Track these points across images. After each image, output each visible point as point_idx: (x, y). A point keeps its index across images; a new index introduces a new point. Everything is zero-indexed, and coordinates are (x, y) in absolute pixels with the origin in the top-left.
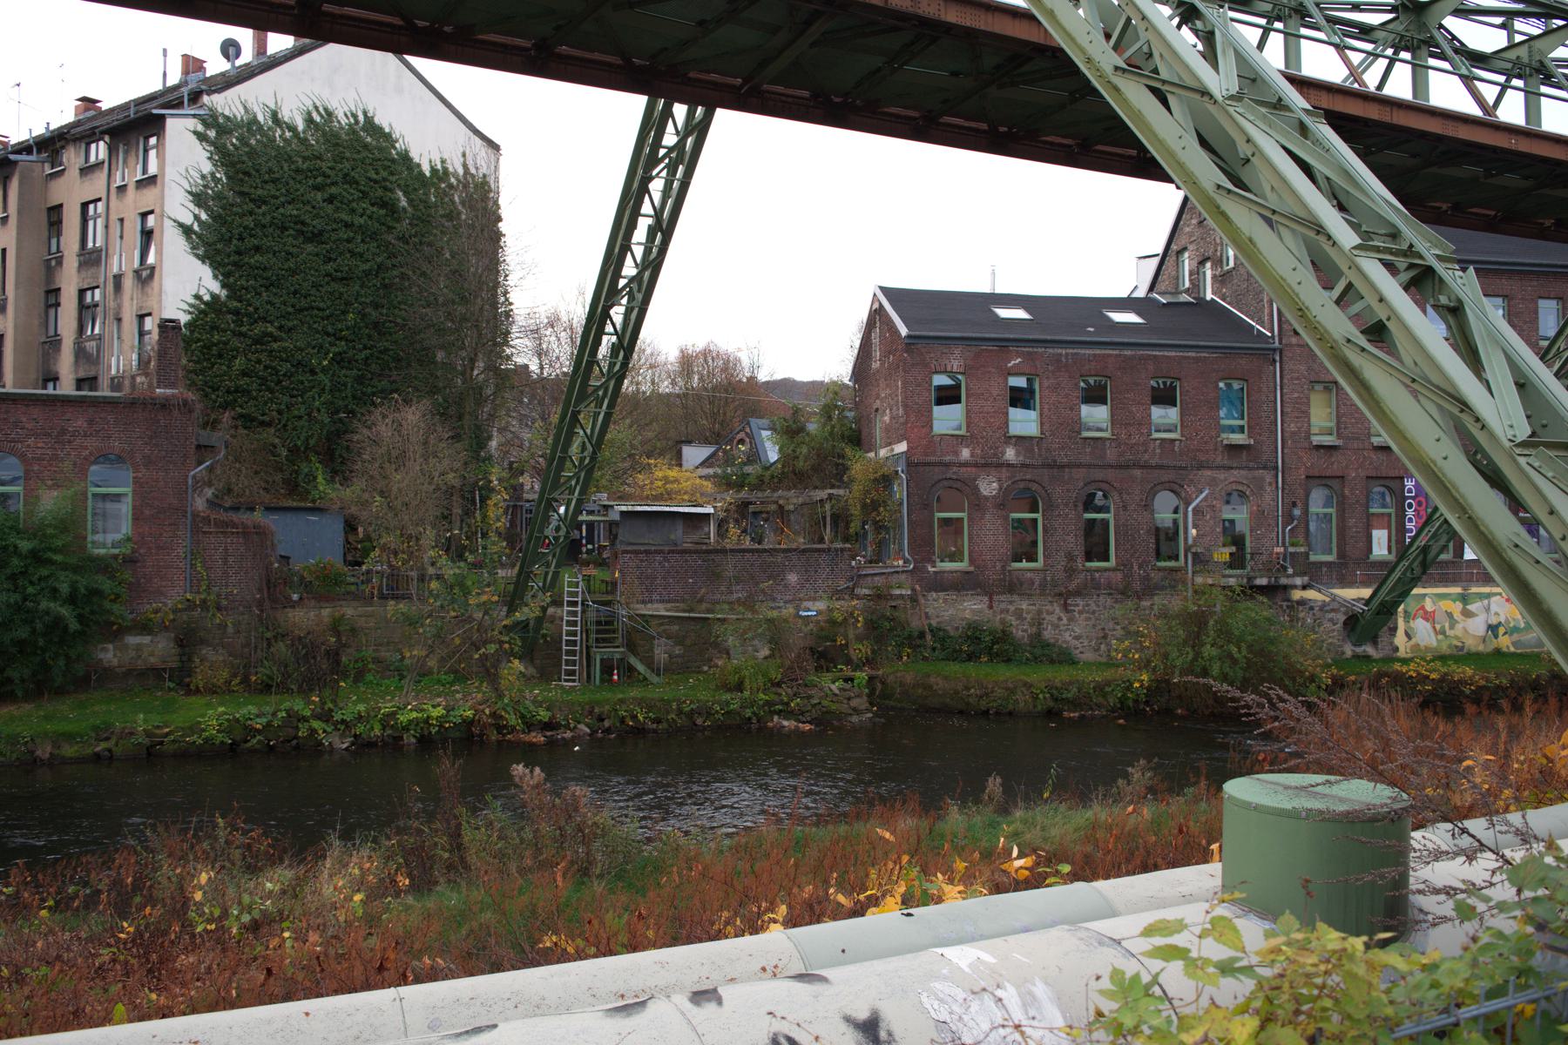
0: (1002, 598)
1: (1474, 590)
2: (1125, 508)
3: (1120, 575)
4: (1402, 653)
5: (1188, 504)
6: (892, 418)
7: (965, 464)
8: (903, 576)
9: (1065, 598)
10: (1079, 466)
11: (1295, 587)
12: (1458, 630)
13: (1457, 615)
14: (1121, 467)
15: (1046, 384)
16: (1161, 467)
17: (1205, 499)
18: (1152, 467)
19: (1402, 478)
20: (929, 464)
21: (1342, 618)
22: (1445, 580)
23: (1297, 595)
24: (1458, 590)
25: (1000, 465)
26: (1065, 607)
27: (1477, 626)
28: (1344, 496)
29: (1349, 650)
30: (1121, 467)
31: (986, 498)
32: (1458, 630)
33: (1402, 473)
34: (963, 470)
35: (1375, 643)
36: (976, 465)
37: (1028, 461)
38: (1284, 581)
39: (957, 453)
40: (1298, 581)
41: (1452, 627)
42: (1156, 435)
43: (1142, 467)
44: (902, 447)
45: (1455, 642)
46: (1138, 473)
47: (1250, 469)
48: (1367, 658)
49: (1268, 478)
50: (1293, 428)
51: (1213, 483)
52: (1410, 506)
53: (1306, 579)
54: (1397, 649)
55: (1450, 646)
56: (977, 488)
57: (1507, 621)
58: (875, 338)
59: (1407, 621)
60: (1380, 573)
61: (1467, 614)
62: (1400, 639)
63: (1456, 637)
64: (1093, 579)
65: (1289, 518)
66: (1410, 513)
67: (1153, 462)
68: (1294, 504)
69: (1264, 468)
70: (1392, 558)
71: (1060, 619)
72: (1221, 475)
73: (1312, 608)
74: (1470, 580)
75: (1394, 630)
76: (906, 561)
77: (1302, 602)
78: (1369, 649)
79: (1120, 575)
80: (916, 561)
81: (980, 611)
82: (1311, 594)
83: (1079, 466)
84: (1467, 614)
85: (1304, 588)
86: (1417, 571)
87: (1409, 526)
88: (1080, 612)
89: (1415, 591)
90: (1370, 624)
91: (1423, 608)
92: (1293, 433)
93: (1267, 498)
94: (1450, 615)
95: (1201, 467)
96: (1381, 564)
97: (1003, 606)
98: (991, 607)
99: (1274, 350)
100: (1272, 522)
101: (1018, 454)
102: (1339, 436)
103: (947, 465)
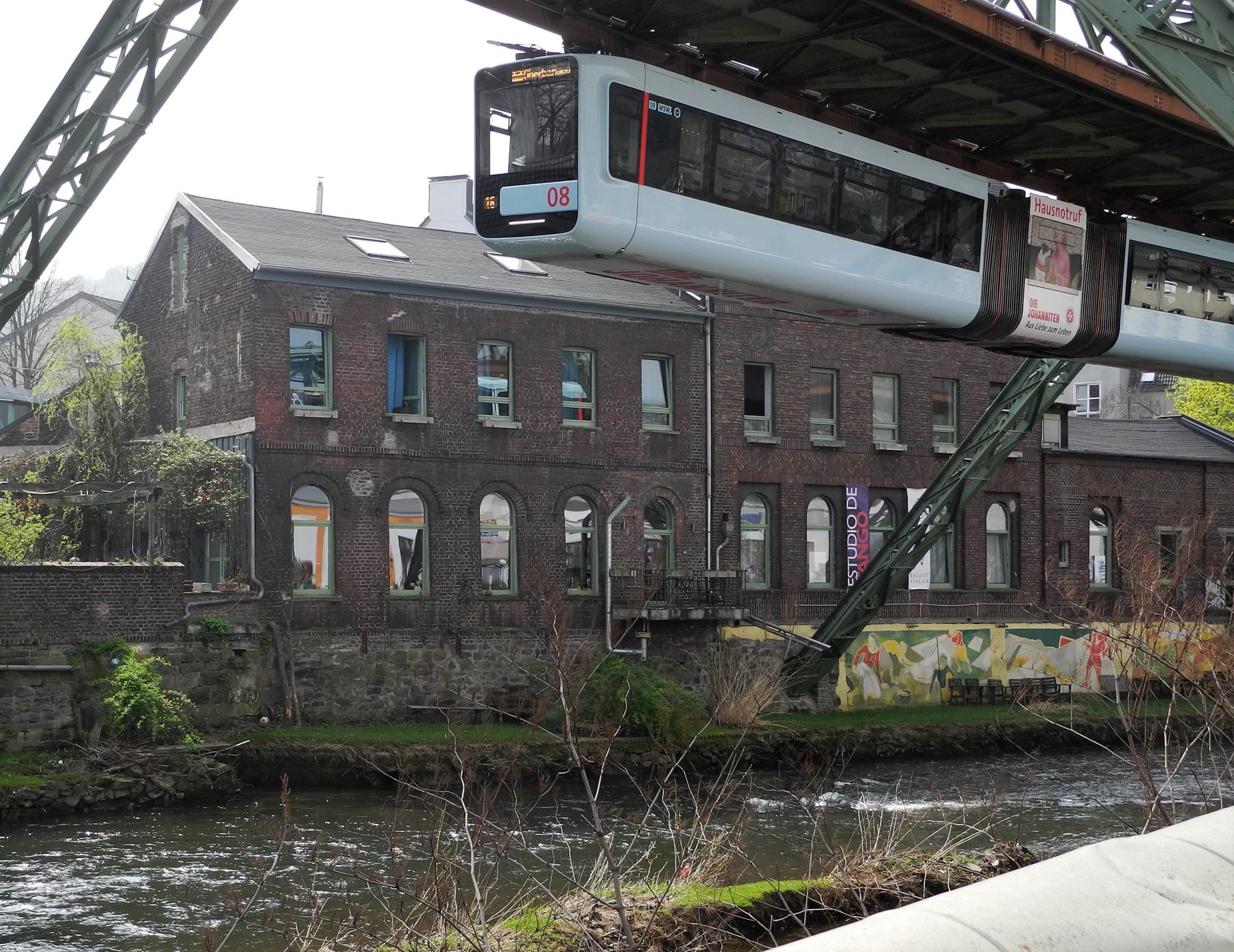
0: (380, 637)
1: (922, 627)
2: (529, 517)
3: (524, 606)
4: (844, 706)
5: (605, 514)
6: (216, 386)
7: (332, 453)
8: (250, 608)
9: (455, 636)
10: (475, 459)
11: (725, 622)
12: (902, 679)
13: (902, 658)
14: (526, 463)
15: (435, 347)
16: (572, 465)
17: (624, 510)
18: (563, 465)
19: (843, 488)
20: (284, 451)
21: (778, 664)
22: (892, 617)
23: (729, 632)
24: (900, 627)
25: (377, 456)
26: (458, 649)
27: (922, 671)
28: (780, 509)
29: (785, 703)
30: (526, 463)
31: (358, 500)
32: (902, 679)
33: (843, 481)
34: (329, 460)
35: (813, 692)
36: (346, 455)
37: (412, 452)
38: (722, 614)
39: (322, 438)
40: (738, 614)
41: (896, 673)
42: (567, 423)
43: (552, 464)
44: (248, 425)
45: (901, 692)
46: (546, 471)
47: (675, 470)
48: (806, 712)
49: (695, 479)
50: (724, 419)
51: (633, 487)
52: (852, 522)
53: (747, 610)
54: (838, 701)
55: (895, 696)
56: (347, 485)
57: (955, 666)
58: (180, 266)
59: (849, 666)
60: (814, 604)
61: (914, 657)
62: (842, 689)
63: (902, 686)
64: (492, 612)
65: (720, 535)
66: (852, 530)
67: (564, 458)
68: (725, 517)
69: (693, 470)
70: (830, 586)
71: (452, 666)
72: (642, 478)
73: (745, 650)
74: (916, 614)
75: (836, 676)
76: (254, 587)
77: (734, 641)
78: (808, 701)
79: (524, 606)
80: (267, 588)
81: (352, 656)
82: (753, 633)
83: (475, 459)
84: (914, 657)
85: (737, 624)
86: (874, 600)
87: (851, 547)
88: (477, 656)
89: (867, 629)
90: (808, 670)
91: (865, 649)
92: (723, 426)
93: (696, 509)
94: (894, 658)
95: (620, 465)
96: (820, 594)
97: (381, 649)
98: (364, 650)
99: (706, 319)
100: (700, 540)
101: (399, 441)
102: (775, 433)
103: (308, 453)
